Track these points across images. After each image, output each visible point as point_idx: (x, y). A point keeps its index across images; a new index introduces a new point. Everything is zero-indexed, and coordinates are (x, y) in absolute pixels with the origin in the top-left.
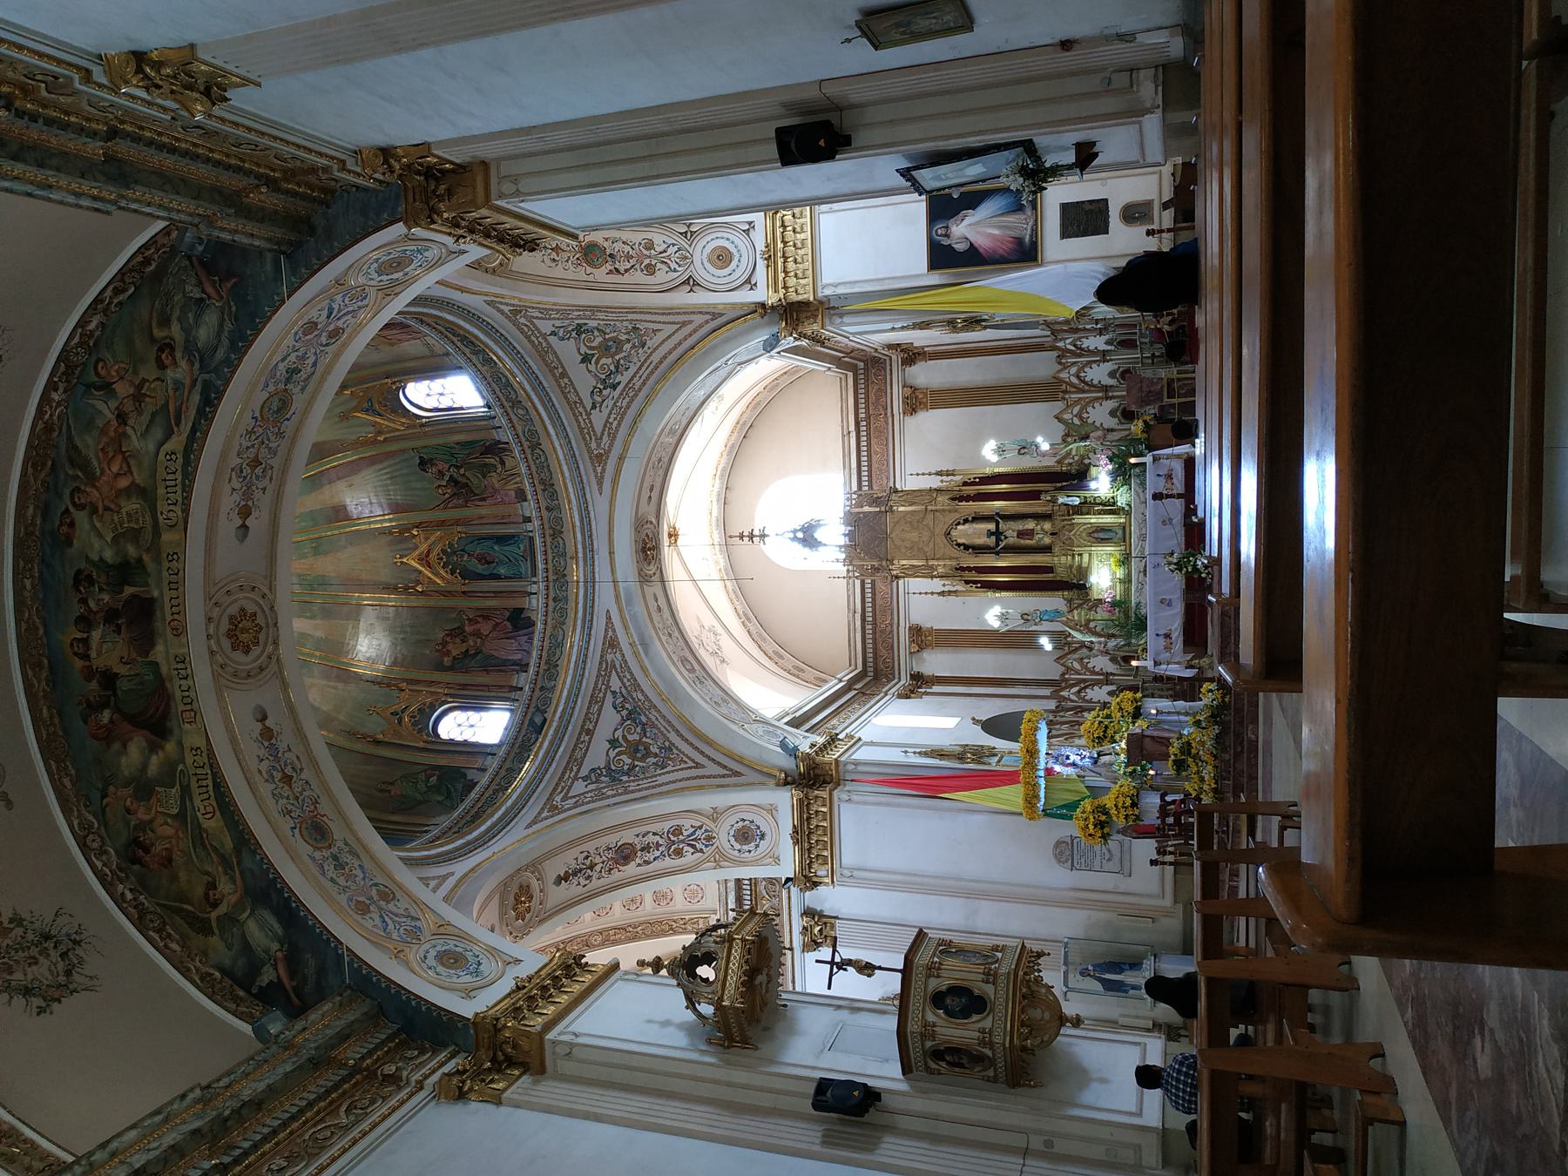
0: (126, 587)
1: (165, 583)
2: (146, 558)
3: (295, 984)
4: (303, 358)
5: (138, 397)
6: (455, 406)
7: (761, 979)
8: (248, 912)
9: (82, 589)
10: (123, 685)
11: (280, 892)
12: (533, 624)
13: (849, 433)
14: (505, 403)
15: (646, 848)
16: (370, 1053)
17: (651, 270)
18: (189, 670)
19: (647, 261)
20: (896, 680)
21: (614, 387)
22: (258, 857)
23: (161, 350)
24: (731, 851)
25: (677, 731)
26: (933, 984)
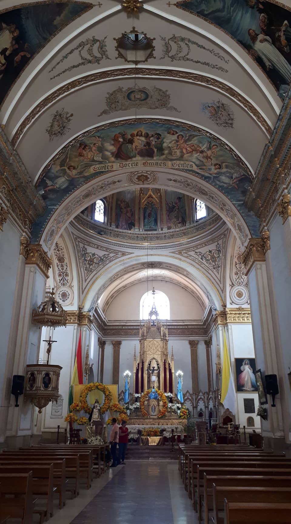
0: (156, 149)
2: (164, 156)
3: (47, 191)
4: (216, 200)
6: (197, 206)
7: (50, 324)
8: (67, 179)
9: (156, 136)
10: (129, 146)
11: (73, 189)
12: (130, 230)
14: (197, 227)
15: (62, 266)
17: (236, 274)
18: (134, 167)
19: (239, 273)
20: (103, 336)
21: (202, 259)
22: (83, 183)
23: (220, 165)
24: (59, 292)
25: (96, 274)
26: (52, 373)
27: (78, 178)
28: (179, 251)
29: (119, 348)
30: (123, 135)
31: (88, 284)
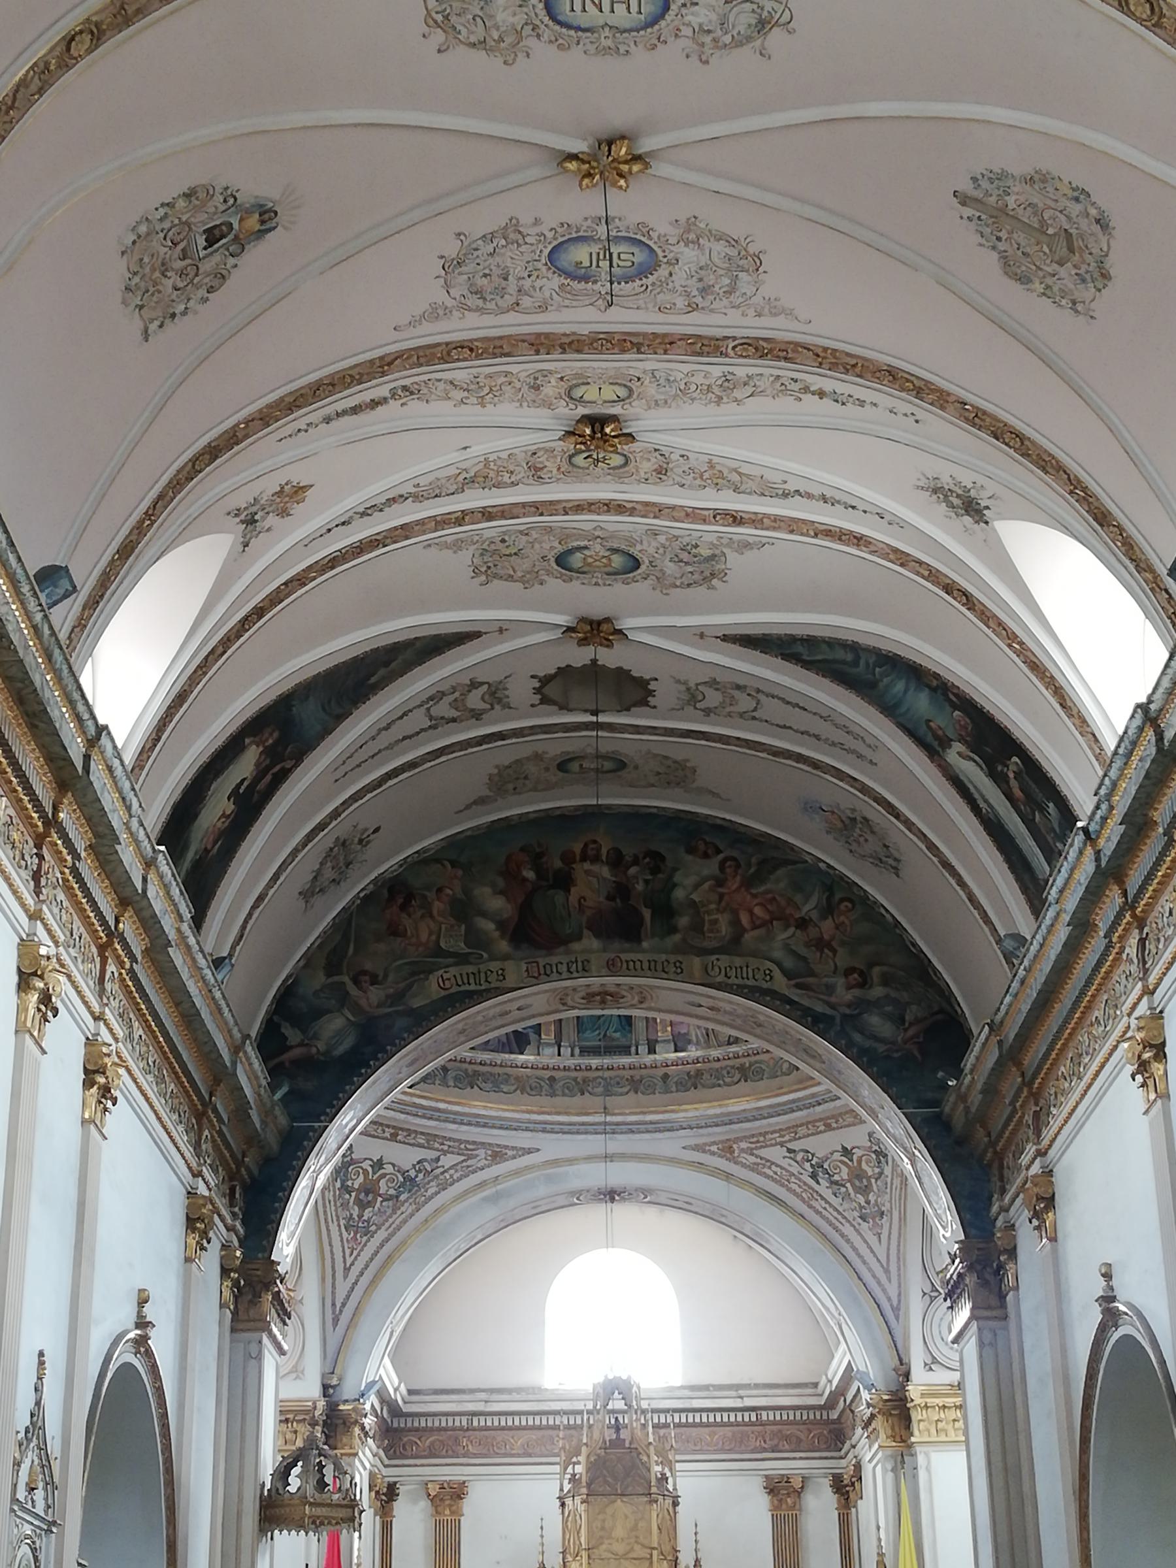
1: (656, 957)
2: (677, 937)
3: (287, 1064)
5: (821, 944)
8: (352, 1018)
9: (647, 860)
10: (559, 897)
12: (522, 1053)
13: (741, 1397)
16: (248, 1169)
18: (575, 975)
20: (387, 1462)
21: (814, 1176)
22: (406, 1035)
23: (862, 973)
25: (387, 1240)
27: (389, 1015)
28: (722, 1142)
29: (457, 1513)
30: (537, 859)
31: (356, 1283)
